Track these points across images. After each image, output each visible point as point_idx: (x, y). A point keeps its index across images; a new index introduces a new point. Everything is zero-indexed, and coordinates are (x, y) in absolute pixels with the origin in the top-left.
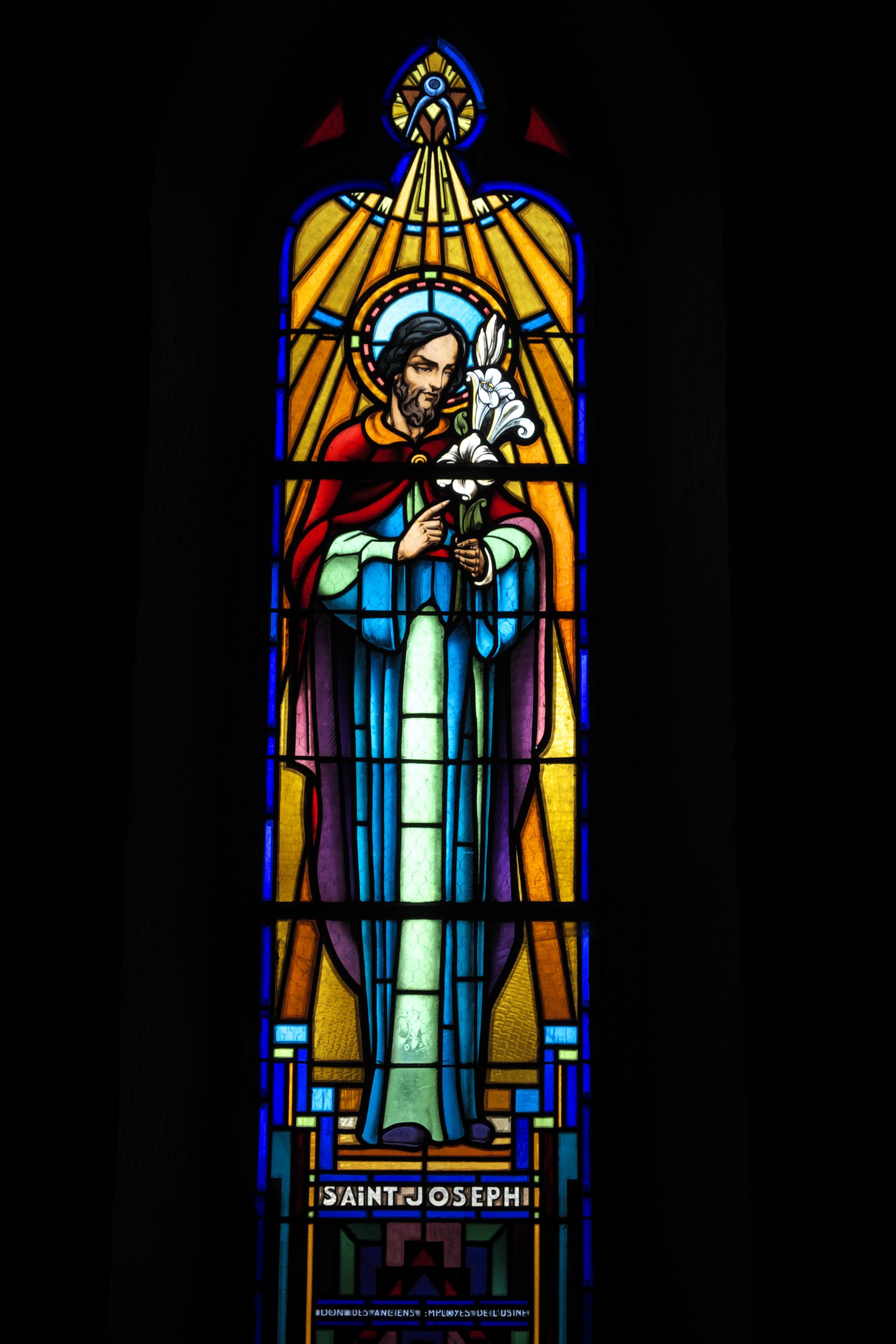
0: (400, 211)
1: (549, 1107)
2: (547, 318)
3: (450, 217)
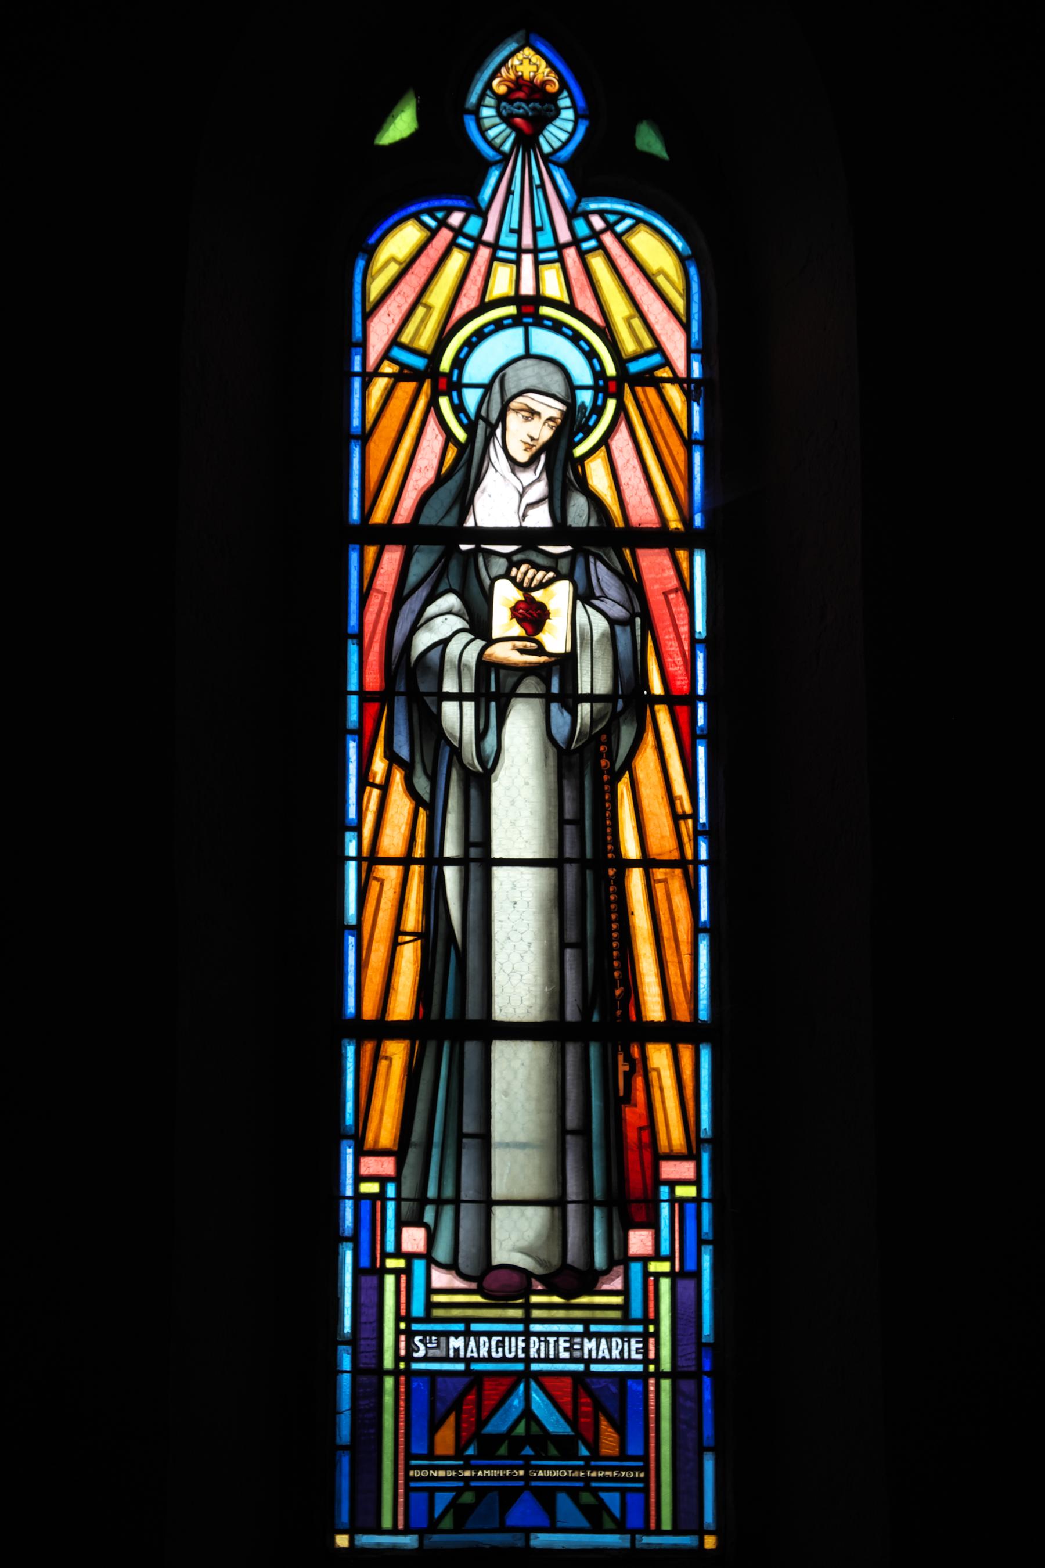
0: (489, 236)
1: (665, 1250)
2: (656, 359)
3: (545, 240)
